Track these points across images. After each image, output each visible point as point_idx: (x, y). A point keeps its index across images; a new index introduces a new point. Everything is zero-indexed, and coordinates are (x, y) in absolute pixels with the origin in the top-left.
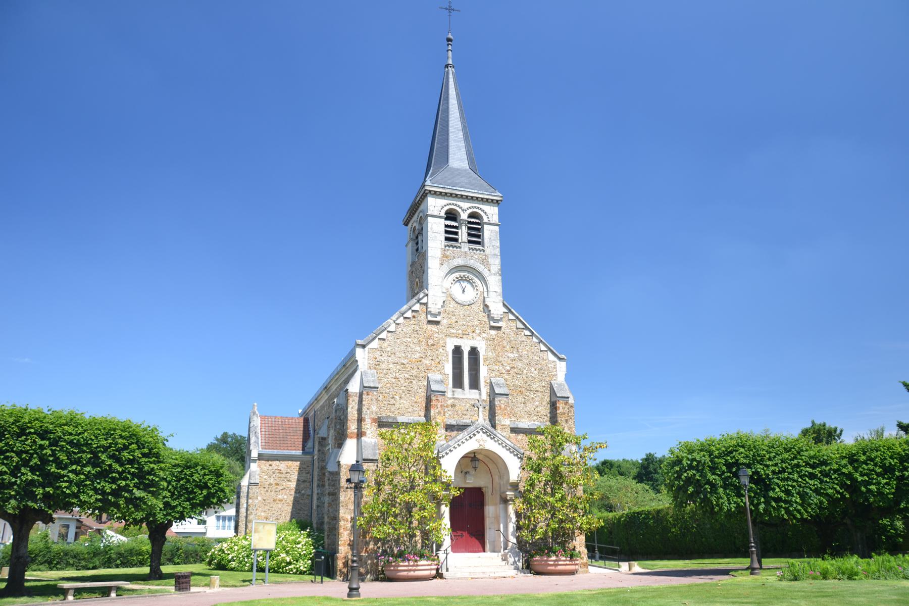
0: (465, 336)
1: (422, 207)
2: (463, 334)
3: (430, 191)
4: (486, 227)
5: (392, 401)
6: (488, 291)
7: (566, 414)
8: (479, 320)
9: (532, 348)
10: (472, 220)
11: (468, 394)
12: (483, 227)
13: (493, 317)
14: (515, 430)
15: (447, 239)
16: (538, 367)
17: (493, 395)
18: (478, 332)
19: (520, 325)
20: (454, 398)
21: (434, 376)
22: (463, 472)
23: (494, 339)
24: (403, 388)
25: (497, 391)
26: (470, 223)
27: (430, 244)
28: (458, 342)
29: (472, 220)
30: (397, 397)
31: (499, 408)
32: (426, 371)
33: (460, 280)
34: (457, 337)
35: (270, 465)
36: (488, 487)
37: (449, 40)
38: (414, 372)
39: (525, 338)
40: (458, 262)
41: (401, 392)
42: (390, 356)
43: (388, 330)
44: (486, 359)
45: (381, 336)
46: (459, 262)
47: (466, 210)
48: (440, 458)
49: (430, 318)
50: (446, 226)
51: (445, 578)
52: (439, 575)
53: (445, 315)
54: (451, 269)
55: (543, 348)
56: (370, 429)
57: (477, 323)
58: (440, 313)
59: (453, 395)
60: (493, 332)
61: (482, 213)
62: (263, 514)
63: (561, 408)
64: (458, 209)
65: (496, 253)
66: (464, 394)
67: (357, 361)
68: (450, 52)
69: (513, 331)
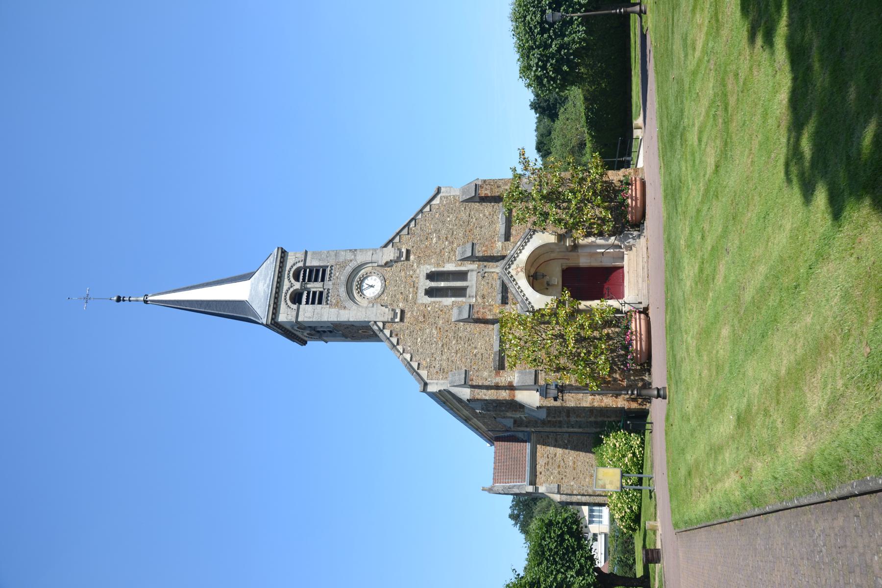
0: (416, 285)
1: (288, 327)
2: (414, 287)
3: (272, 319)
4: (308, 264)
5: (479, 356)
6: (372, 263)
7: (492, 187)
8: (400, 271)
10: (301, 278)
11: (472, 282)
12: (308, 267)
13: (397, 257)
14: (507, 237)
15: (320, 303)
16: (446, 214)
17: (473, 258)
18: (411, 273)
19: (405, 231)
21: (455, 315)
22: (547, 287)
23: (419, 257)
24: (466, 346)
25: (469, 254)
26: (304, 280)
27: (325, 319)
28: (421, 292)
29: (301, 278)
30: (475, 351)
31: (486, 252)
32: (450, 323)
33: (360, 289)
34: (416, 293)
35: (541, 473)
36: (562, 264)
37: (119, 299)
38: (451, 335)
39: (418, 227)
41: (470, 347)
42: (435, 359)
43: (409, 360)
44: (438, 265)
45: (416, 367)
46: (342, 290)
47: (292, 284)
48: (533, 309)
49: (397, 320)
50: (307, 303)
51: (648, 305)
52: (645, 311)
53: (395, 304)
54: (350, 299)
55: (427, 209)
56: (505, 378)
57: (403, 274)
58: (393, 310)
59: (473, 297)
60: (412, 257)
61: (295, 268)
62: (587, 480)
63: (486, 192)
64: (290, 292)
65: (334, 254)
66: (472, 286)
67: (440, 391)
68: (131, 299)
69: (411, 238)
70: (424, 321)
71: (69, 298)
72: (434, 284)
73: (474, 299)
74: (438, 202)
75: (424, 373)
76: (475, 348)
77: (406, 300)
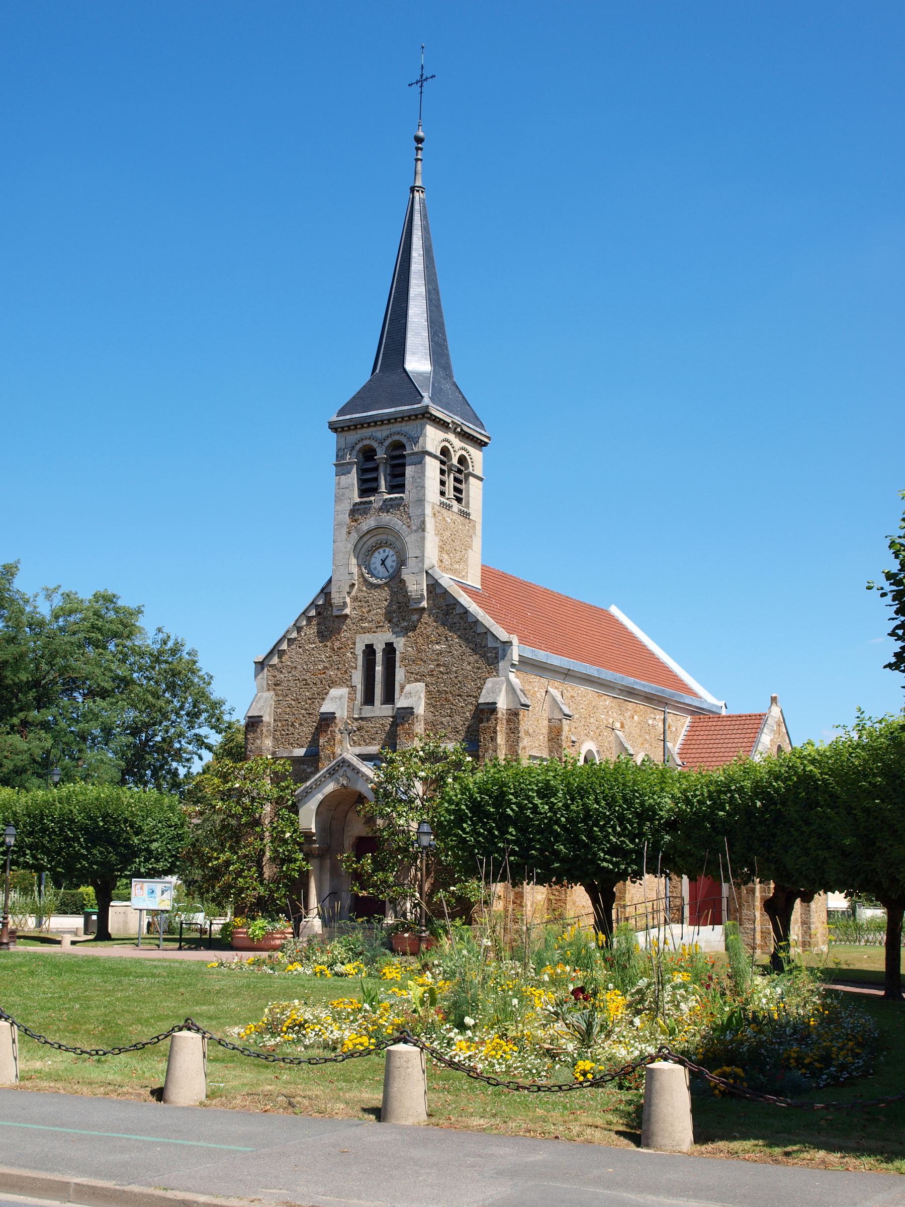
0: (379, 629)
9: (467, 631)
20: (361, 719)
28: (367, 638)
37: (419, 140)
40: (370, 524)
44: (403, 659)
54: (361, 538)
59: (360, 713)
70: (334, 650)
71: (423, 48)
72: (379, 657)
73: (357, 716)
74: (490, 645)
75: (275, 660)
76: (301, 724)
77: (362, 619)
